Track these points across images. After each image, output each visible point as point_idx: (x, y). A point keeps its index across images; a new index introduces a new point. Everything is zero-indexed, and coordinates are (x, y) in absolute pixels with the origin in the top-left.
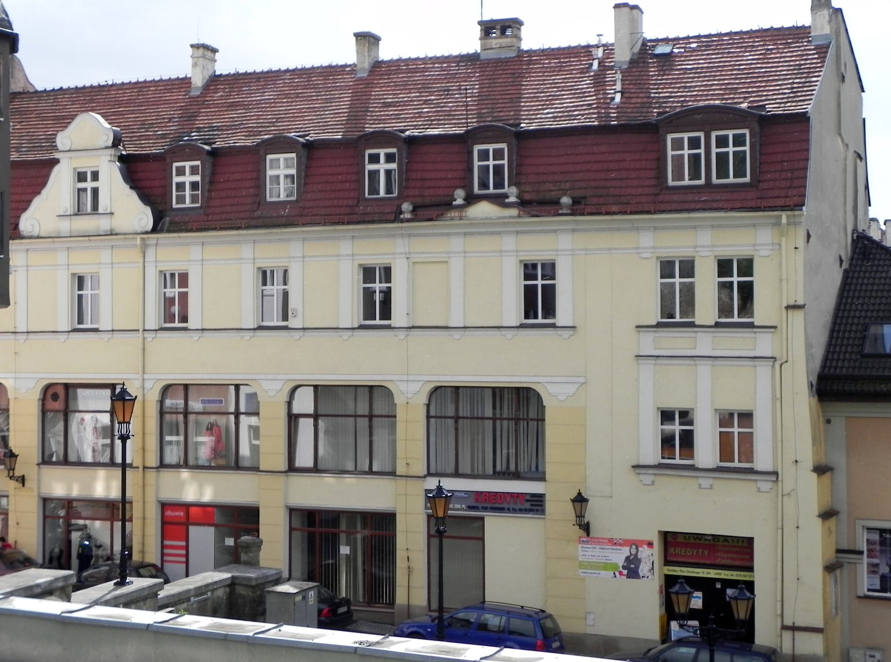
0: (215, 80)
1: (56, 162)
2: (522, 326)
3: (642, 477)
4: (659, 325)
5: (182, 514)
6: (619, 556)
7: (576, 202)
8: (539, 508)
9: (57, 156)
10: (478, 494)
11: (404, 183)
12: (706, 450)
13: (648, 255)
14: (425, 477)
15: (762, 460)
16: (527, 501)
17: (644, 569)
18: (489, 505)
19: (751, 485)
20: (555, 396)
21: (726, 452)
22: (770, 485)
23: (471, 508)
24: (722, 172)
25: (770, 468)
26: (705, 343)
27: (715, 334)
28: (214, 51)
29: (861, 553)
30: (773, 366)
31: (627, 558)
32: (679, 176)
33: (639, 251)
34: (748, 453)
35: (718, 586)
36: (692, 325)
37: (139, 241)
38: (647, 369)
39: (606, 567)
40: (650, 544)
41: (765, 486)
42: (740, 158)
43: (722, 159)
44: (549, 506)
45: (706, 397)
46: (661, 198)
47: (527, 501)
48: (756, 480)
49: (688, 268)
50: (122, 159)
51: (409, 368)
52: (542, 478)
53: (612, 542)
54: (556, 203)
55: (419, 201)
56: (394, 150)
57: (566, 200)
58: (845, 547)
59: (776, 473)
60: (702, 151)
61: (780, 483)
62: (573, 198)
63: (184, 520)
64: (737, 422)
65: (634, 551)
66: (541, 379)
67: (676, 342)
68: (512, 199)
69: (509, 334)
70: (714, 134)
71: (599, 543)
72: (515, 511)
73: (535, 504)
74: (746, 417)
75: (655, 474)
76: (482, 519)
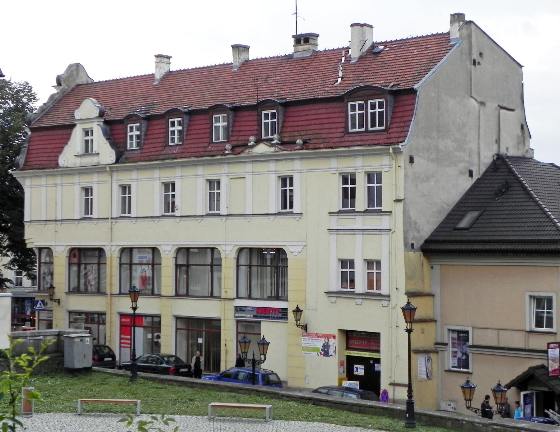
0: (170, 74)
1: (75, 125)
2: (279, 214)
3: (331, 298)
5: (129, 320)
6: (319, 344)
7: (305, 142)
9: (75, 123)
11: (230, 133)
13: (334, 172)
17: (331, 351)
23: (255, 316)
26: (359, 222)
27: (365, 217)
28: (169, 58)
29: (446, 344)
31: (324, 344)
32: (353, 126)
35: (372, 362)
36: (354, 211)
37: (108, 169)
38: (334, 237)
47: (280, 312)
50: (106, 122)
51: (228, 238)
52: (287, 300)
53: (317, 336)
54: (294, 143)
55: (235, 143)
56: (275, 111)
57: (299, 141)
58: (439, 341)
62: (303, 140)
63: (129, 324)
65: (327, 341)
66: (286, 243)
67: (347, 222)
68: (275, 141)
69: (272, 218)
71: (311, 336)
72: (274, 318)
73: (282, 314)
75: (337, 297)
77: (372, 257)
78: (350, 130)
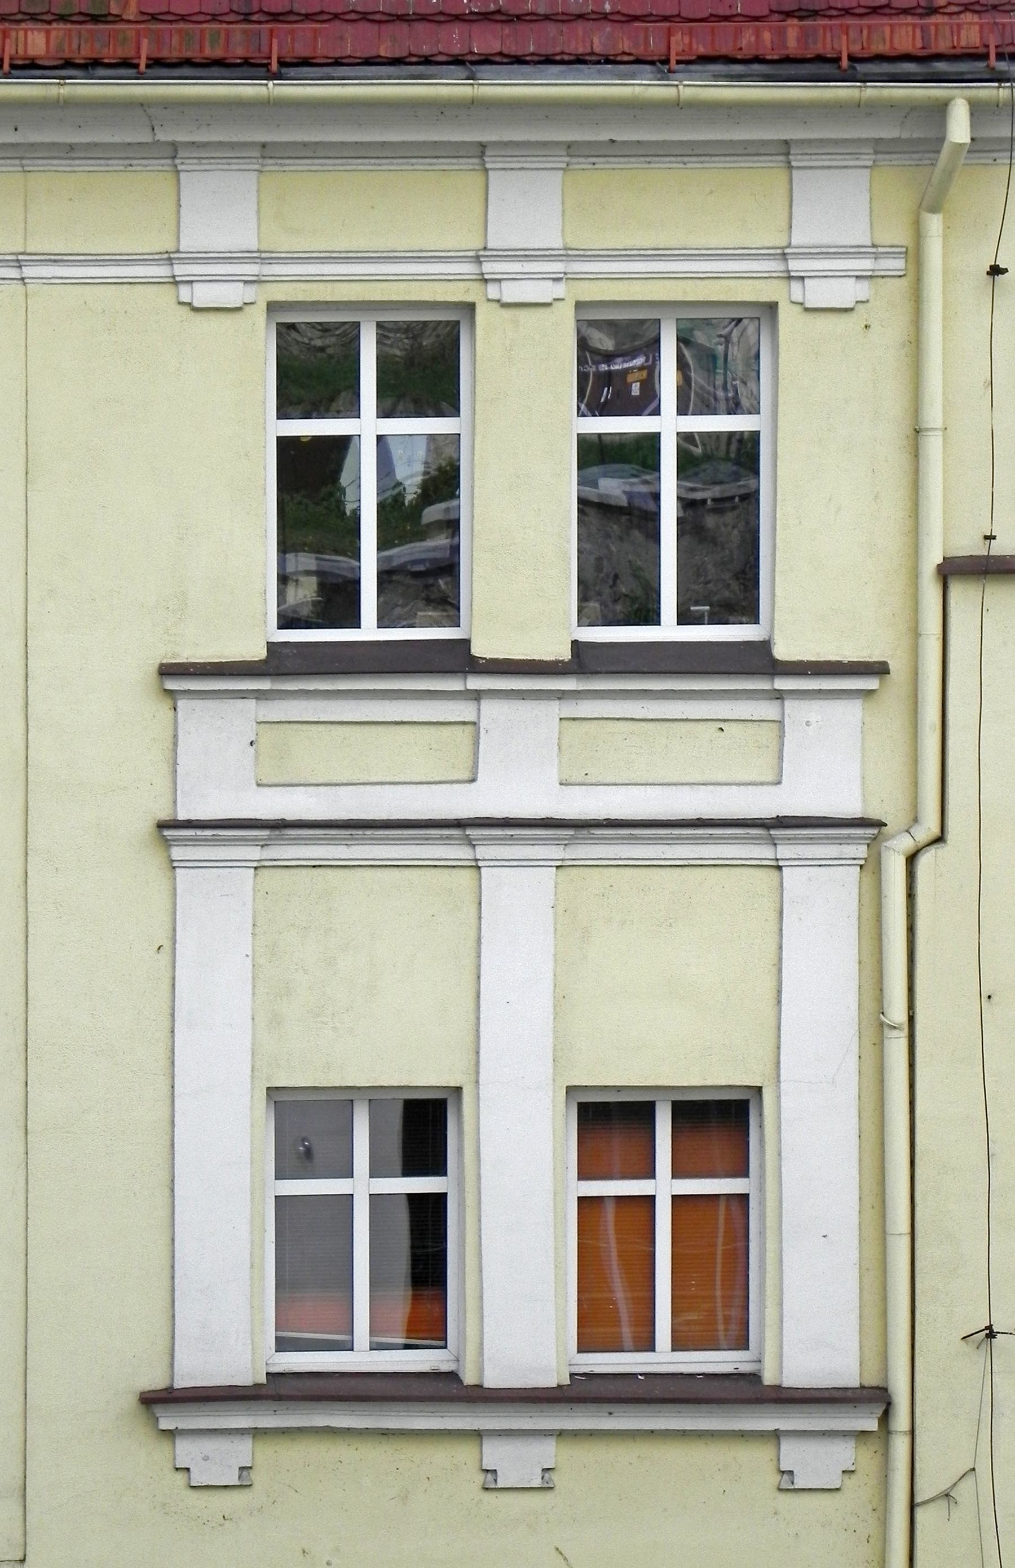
3: (186, 1451)
4: (280, 663)
12: (518, 1298)
13: (231, 295)
19: (756, 1458)
22: (844, 1453)
26: (524, 758)
30: (872, 867)
33: (181, 270)
38: (221, 896)
48: (776, 1435)
59: (876, 1397)
61: (900, 1446)
64: (673, 1142)
67: (373, 750)
74: (720, 1122)
75: (256, 1433)
77: (667, 1057)
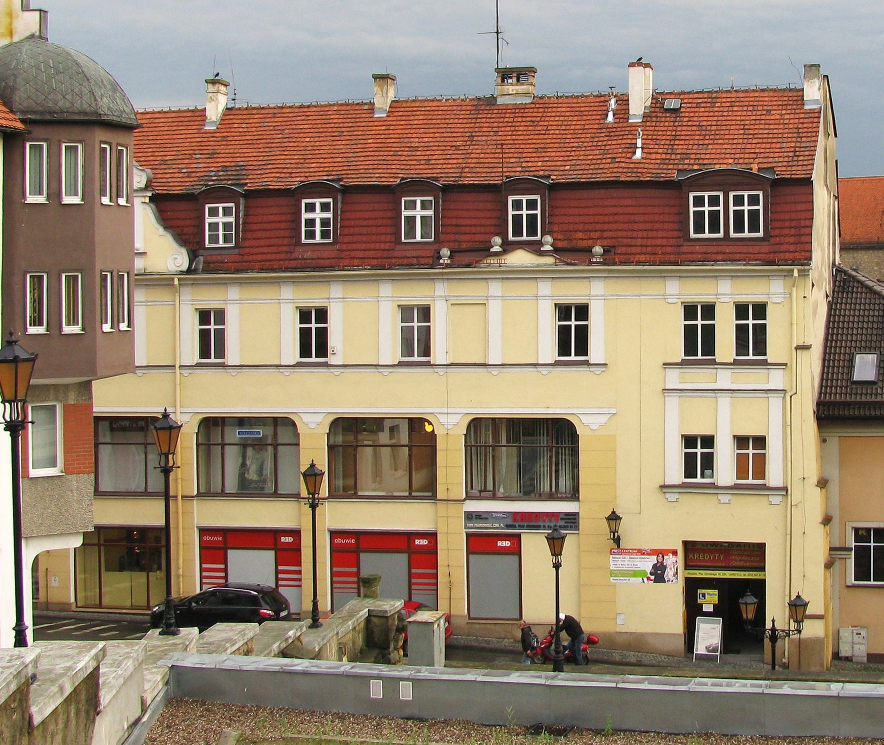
3: (668, 495)
8: (573, 525)
10: (515, 515)
13: (675, 301)
14: (465, 500)
15: (774, 478)
16: (562, 519)
18: (526, 524)
20: (588, 426)
21: (741, 472)
22: (780, 498)
23: (508, 527)
24: (739, 228)
25: (780, 485)
26: (724, 378)
30: (784, 398)
34: (760, 472)
38: (673, 401)
39: (635, 574)
40: (675, 553)
41: (776, 499)
42: (754, 214)
43: (739, 215)
44: (582, 523)
45: (724, 423)
46: (684, 249)
47: (562, 519)
49: (709, 311)
54: (589, 250)
55: (456, 246)
57: (598, 250)
60: (721, 208)
64: (751, 445)
67: (699, 377)
70: (731, 195)
74: (760, 442)
76: (519, 536)
77: (750, 430)
78: (693, 235)
